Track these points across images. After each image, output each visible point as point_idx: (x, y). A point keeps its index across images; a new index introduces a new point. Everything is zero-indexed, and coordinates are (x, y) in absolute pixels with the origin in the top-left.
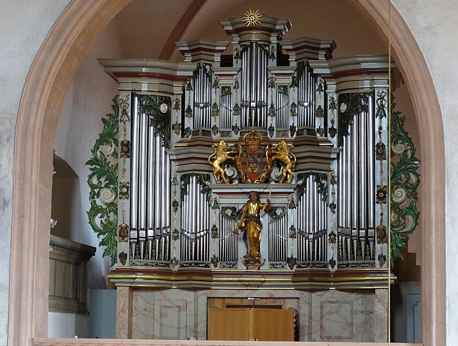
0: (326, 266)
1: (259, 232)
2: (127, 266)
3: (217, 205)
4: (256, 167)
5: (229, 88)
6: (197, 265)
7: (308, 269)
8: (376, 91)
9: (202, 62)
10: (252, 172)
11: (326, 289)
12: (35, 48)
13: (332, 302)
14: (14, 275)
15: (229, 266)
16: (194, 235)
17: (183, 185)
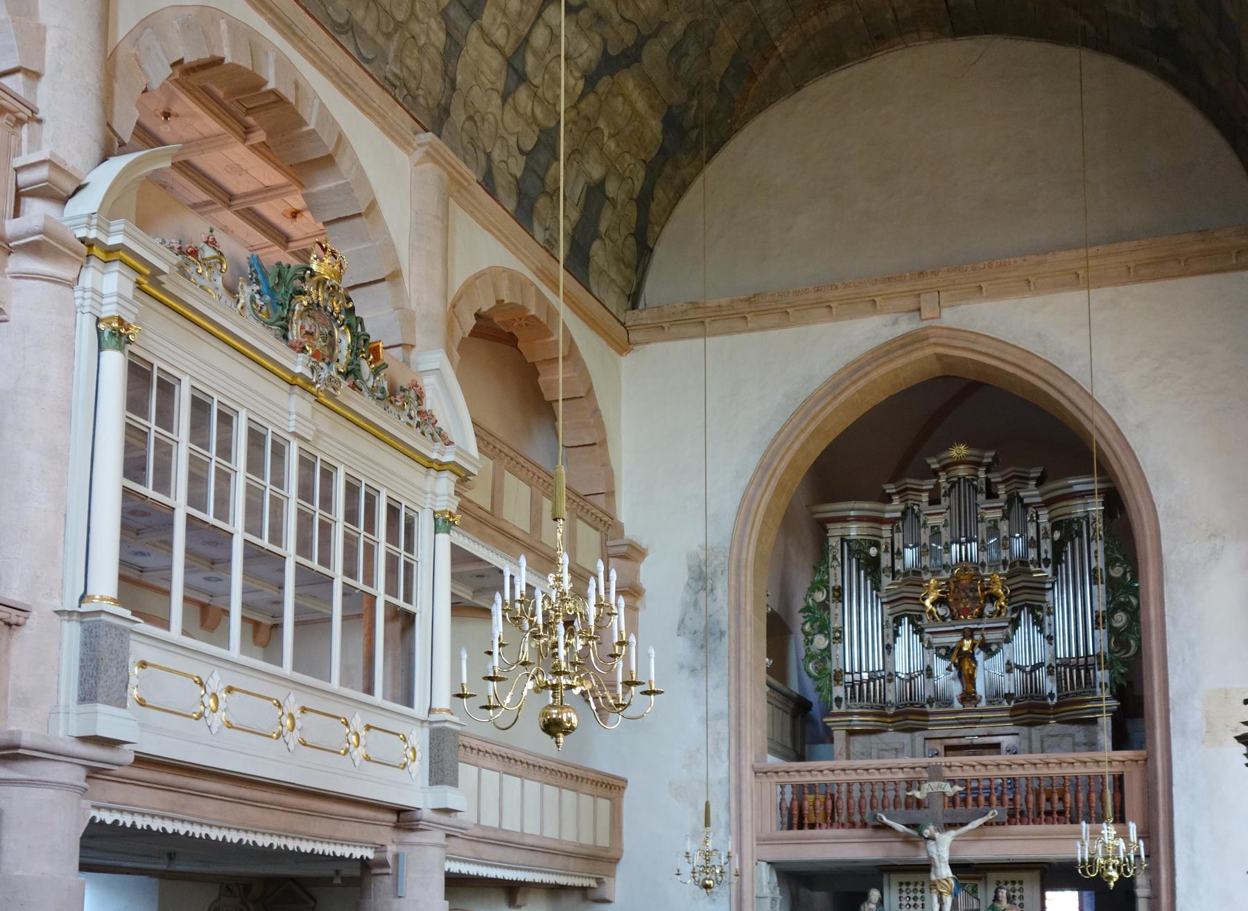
0: (1044, 699)
2: (843, 709)
9: (910, 502)
11: (1044, 722)
12: (744, 482)
13: (1053, 736)
14: (733, 704)
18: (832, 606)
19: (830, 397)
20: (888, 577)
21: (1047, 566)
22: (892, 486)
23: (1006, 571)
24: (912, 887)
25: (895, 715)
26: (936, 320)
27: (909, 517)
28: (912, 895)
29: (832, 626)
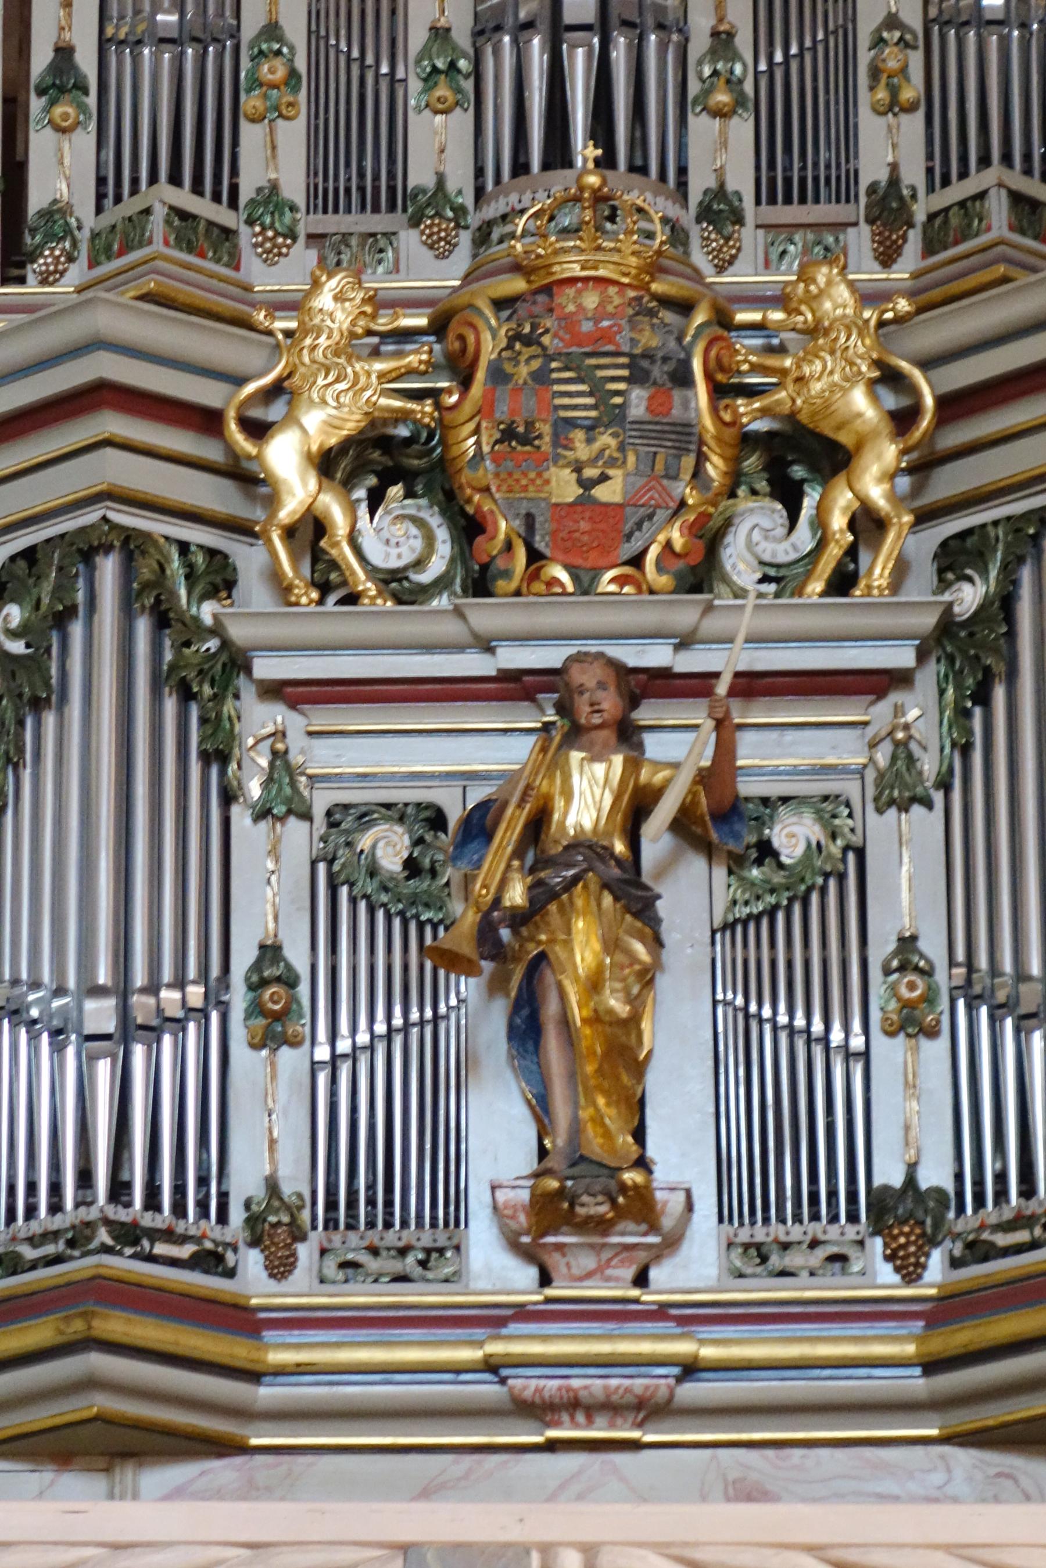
1: (647, 977)
3: (293, 784)
4: (612, 462)
6: (136, 1242)
10: (586, 502)
15: (396, 1266)
16: (110, 1003)
17: (13, 634)
23: (901, 273)
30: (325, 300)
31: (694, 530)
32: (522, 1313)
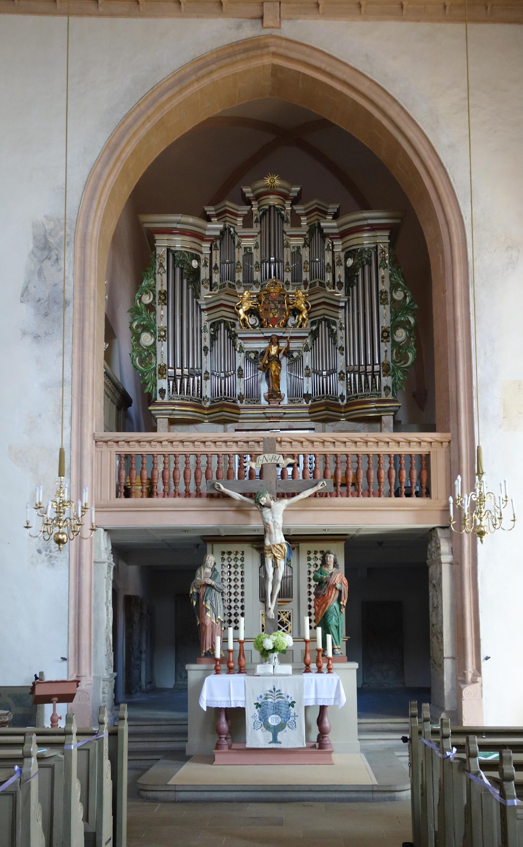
0: (337, 400)
1: (280, 371)
2: (166, 400)
5: (250, 248)
7: (323, 401)
8: (378, 246)
10: (274, 317)
18: (158, 308)
19: (177, 89)
20: (207, 288)
21: (340, 289)
22: (212, 208)
23: (307, 291)
24: (233, 556)
25: (210, 408)
26: (277, 30)
27: (227, 237)
28: (233, 563)
29: (157, 325)
30: (245, 294)
31: (285, 321)
32: (267, 407)
